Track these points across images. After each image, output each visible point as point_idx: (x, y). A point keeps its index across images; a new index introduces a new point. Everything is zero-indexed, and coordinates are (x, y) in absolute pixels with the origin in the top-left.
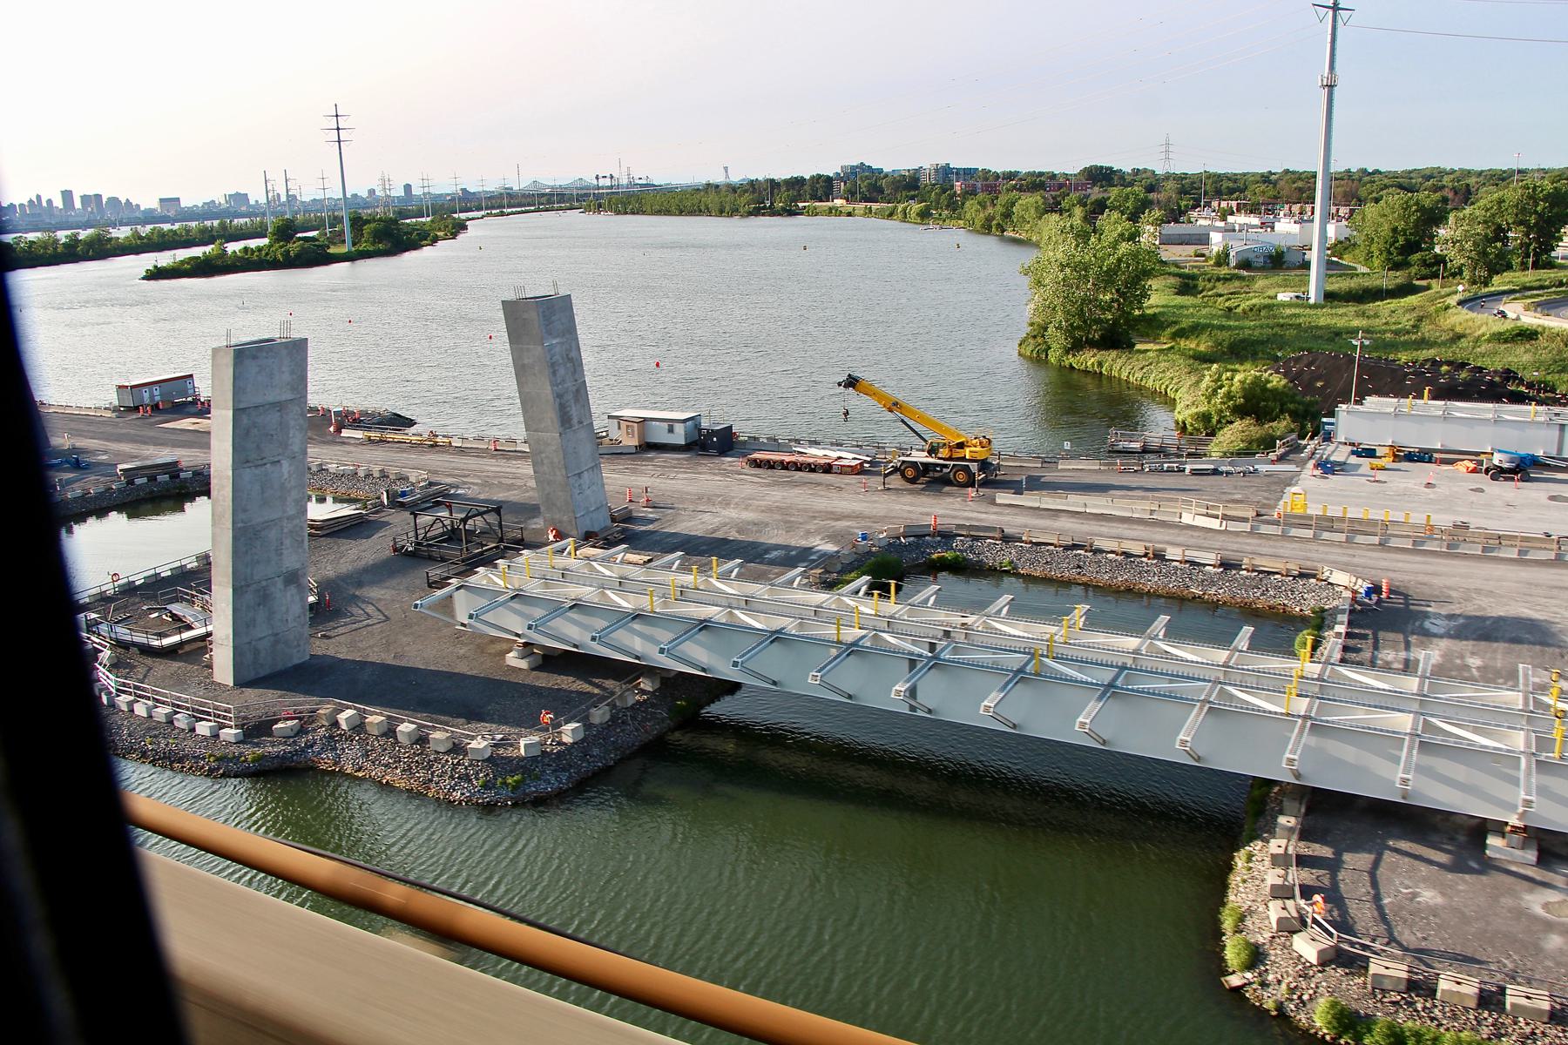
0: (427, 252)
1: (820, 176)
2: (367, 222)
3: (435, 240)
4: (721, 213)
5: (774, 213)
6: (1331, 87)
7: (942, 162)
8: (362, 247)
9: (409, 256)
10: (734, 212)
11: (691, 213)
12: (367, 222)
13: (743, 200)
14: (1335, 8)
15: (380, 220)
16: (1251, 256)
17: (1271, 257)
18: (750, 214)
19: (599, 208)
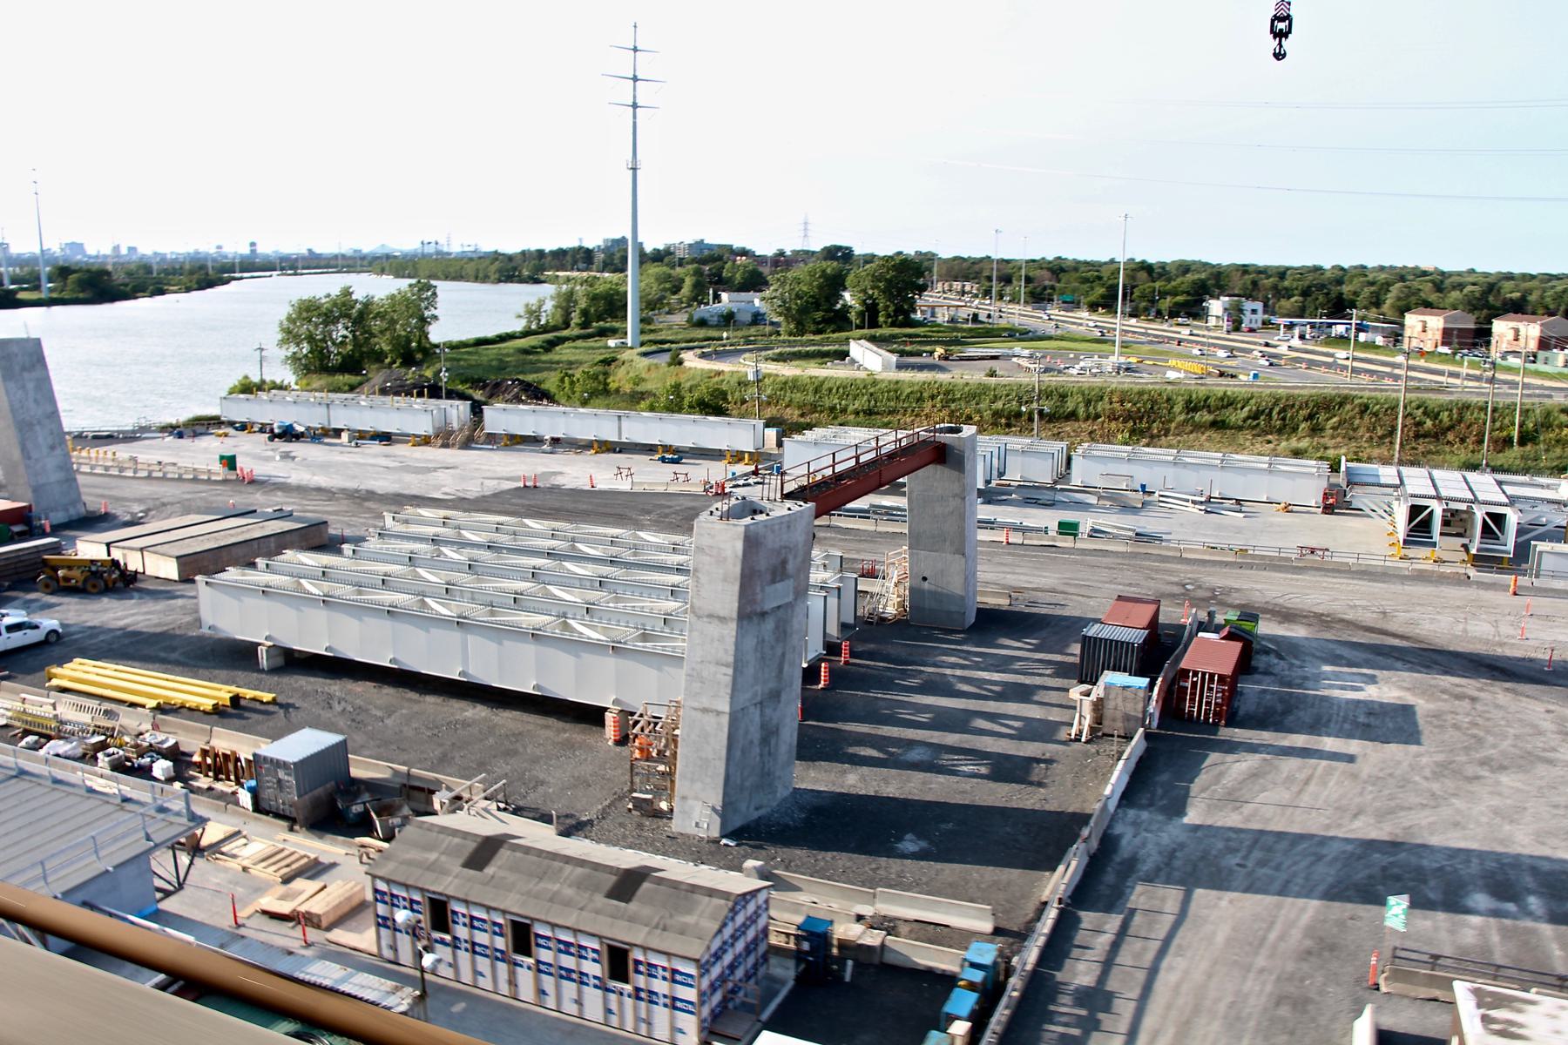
0: (143, 304)
1: (581, 248)
2: (75, 272)
3: (162, 292)
4: (476, 279)
5: (522, 281)
6: (634, 169)
7: (698, 238)
8: (66, 295)
9: (119, 305)
10: (484, 279)
11: (454, 279)
12: (75, 272)
13: (494, 268)
14: (635, 106)
15: (88, 271)
16: (707, 316)
17: (722, 316)
18: (500, 281)
19: (382, 272)
